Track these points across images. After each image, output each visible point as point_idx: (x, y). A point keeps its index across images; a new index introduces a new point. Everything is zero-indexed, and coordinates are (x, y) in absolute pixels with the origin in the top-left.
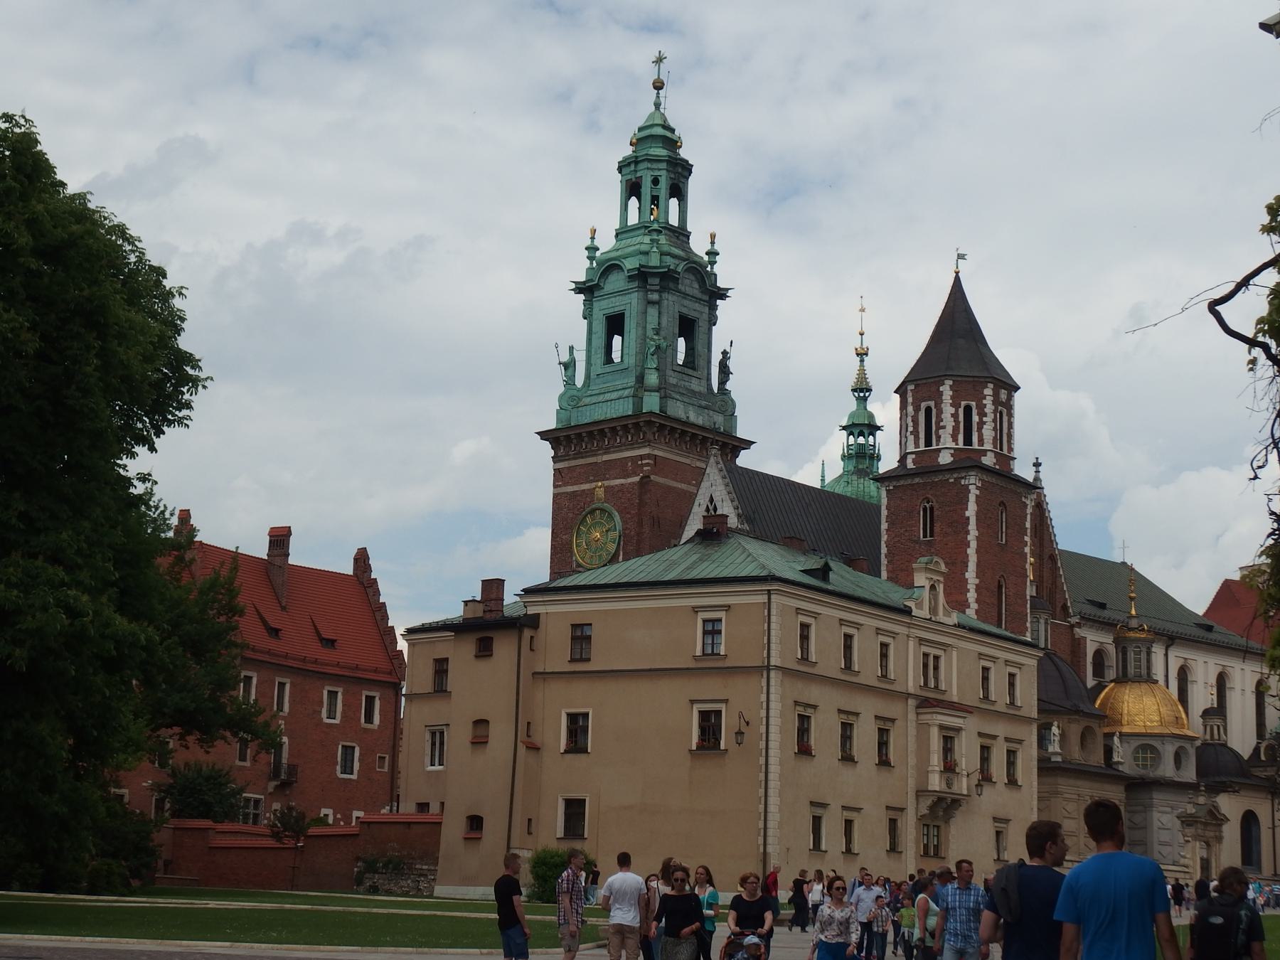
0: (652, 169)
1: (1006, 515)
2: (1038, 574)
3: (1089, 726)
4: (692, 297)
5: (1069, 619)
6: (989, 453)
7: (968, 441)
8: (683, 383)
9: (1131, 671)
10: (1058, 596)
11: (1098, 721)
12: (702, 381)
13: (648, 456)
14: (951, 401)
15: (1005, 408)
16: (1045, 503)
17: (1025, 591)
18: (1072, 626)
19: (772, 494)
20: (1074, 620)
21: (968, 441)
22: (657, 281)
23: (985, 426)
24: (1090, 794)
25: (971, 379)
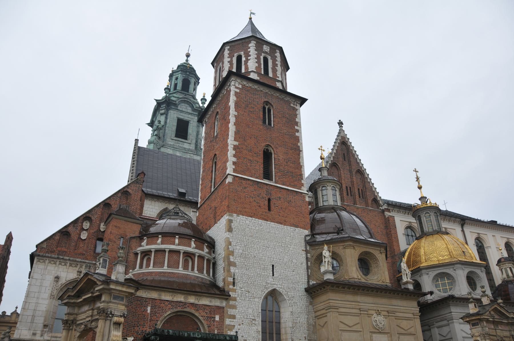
0: (175, 75)
1: (273, 111)
2: (350, 180)
4: (187, 112)
5: (381, 208)
6: (252, 74)
8: (178, 144)
9: (426, 229)
10: (368, 193)
11: (379, 249)
12: (191, 145)
14: (228, 56)
16: (348, 142)
17: (299, 160)
18: (383, 211)
20: (385, 207)
22: (165, 105)
23: (249, 61)
24: (375, 308)
25: (241, 42)
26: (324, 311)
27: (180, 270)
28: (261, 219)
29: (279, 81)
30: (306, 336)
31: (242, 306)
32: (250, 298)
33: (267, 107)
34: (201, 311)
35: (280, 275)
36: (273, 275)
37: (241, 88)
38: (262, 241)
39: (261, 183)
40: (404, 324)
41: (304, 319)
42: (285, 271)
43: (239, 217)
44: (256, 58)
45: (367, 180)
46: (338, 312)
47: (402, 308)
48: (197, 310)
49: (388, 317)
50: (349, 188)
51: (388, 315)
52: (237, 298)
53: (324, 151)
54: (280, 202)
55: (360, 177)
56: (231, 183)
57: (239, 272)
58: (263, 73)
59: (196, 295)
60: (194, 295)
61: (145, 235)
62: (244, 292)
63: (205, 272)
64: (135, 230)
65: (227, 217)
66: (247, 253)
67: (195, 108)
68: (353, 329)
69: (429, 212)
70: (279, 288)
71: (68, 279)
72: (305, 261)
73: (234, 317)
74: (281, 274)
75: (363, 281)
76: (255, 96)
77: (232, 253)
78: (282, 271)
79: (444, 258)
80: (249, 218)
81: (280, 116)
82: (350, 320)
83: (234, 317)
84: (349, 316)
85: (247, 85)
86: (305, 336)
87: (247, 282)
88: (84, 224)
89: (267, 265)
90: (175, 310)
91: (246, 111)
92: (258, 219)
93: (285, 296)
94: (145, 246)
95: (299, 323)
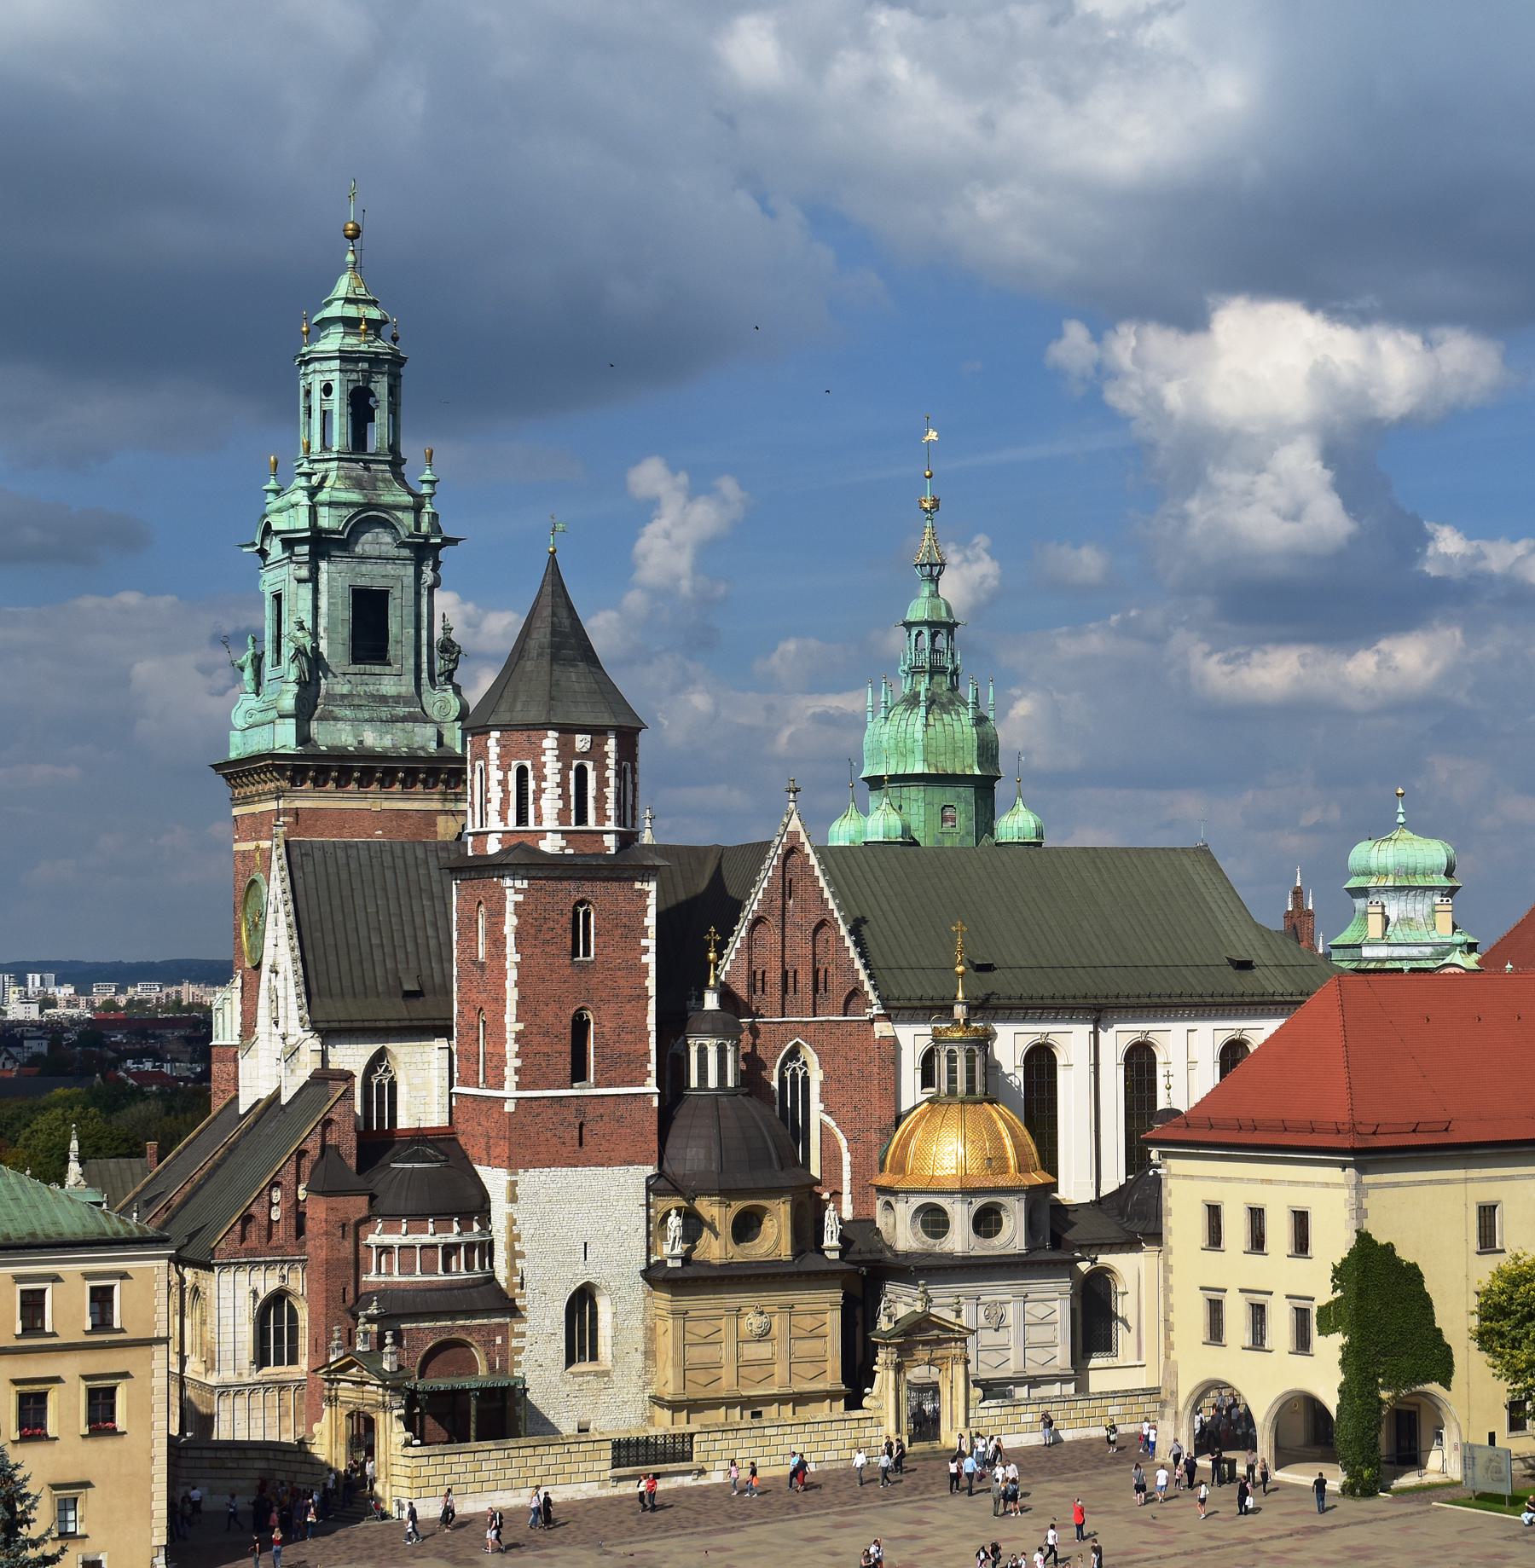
7: (522, 818)
13: (285, 812)
14: (498, 762)
15: (628, 751)
18: (872, 1021)
19: (389, 874)
20: (875, 1010)
21: (522, 818)
22: (305, 549)
26: (664, 1313)
27: (441, 1277)
29: (608, 832)
33: (581, 910)
44: (558, 787)
54: (601, 1124)
61: (380, 1216)
63: (477, 1266)
65: (509, 1178)
67: (403, 537)
68: (709, 1340)
71: (269, 1290)
73: (523, 1335)
77: (517, 1238)
78: (601, 1250)
80: (546, 1170)
83: (523, 1335)
88: (274, 1194)
90: (439, 1339)
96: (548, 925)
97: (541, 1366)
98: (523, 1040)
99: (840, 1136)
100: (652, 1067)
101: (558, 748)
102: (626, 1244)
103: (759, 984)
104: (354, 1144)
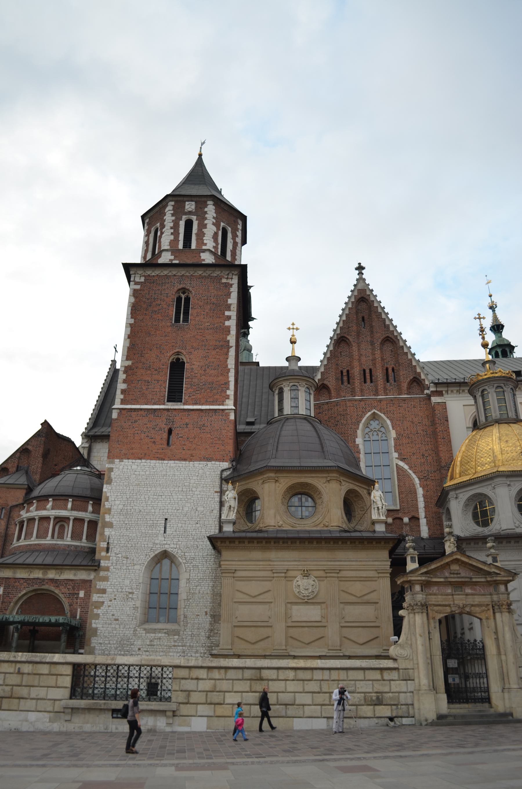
2: (371, 358)
3: (306, 485)
6: (164, 254)
10: (401, 373)
16: (371, 296)
18: (429, 397)
20: (432, 389)
23: (163, 235)
24: (300, 568)
27: (48, 541)
28: (155, 460)
29: (204, 251)
30: (208, 610)
31: (116, 576)
32: (128, 565)
34: (61, 587)
35: (176, 531)
36: (165, 532)
37: (143, 281)
38: (154, 489)
39: (160, 409)
40: (357, 588)
41: (207, 588)
42: (183, 525)
43: (122, 463)
44: (171, 228)
45: (401, 351)
46: (234, 577)
47: (354, 563)
48: (58, 587)
49: (325, 579)
50: (368, 371)
51: (325, 575)
52: (112, 567)
53: (297, 329)
55: (390, 349)
56: (116, 419)
57: (117, 534)
58: (181, 246)
59: (58, 569)
60: (54, 569)
62: (121, 558)
64: (19, 496)
66: (129, 508)
69: (486, 387)
70: (172, 548)
72: (217, 507)
73: (103, 591)
74: (177, 530)
75: (287, 528)
76: (163, 287)
78: (180, 525)
79: (484, 468)
81: (201, 304)
82: (254, 588)
83: (103, 591)
84: (253, 582)
85: (153, 274)
86: (206, 610)
87: (125, 545)
89: (157, 519)
90: (31, 588)
91: (147, 312)
92: (151, 459)
93: (179, 559)
94: (24, 515)
95: (199, 593)
96: (157, 302)
97: (117, 620)
98: (130, 372)
99: (414, 476)
100: (231, 392)
101: (173, 210)
102: (201, 522)
103: (345, 378)
104: (40, 465)
